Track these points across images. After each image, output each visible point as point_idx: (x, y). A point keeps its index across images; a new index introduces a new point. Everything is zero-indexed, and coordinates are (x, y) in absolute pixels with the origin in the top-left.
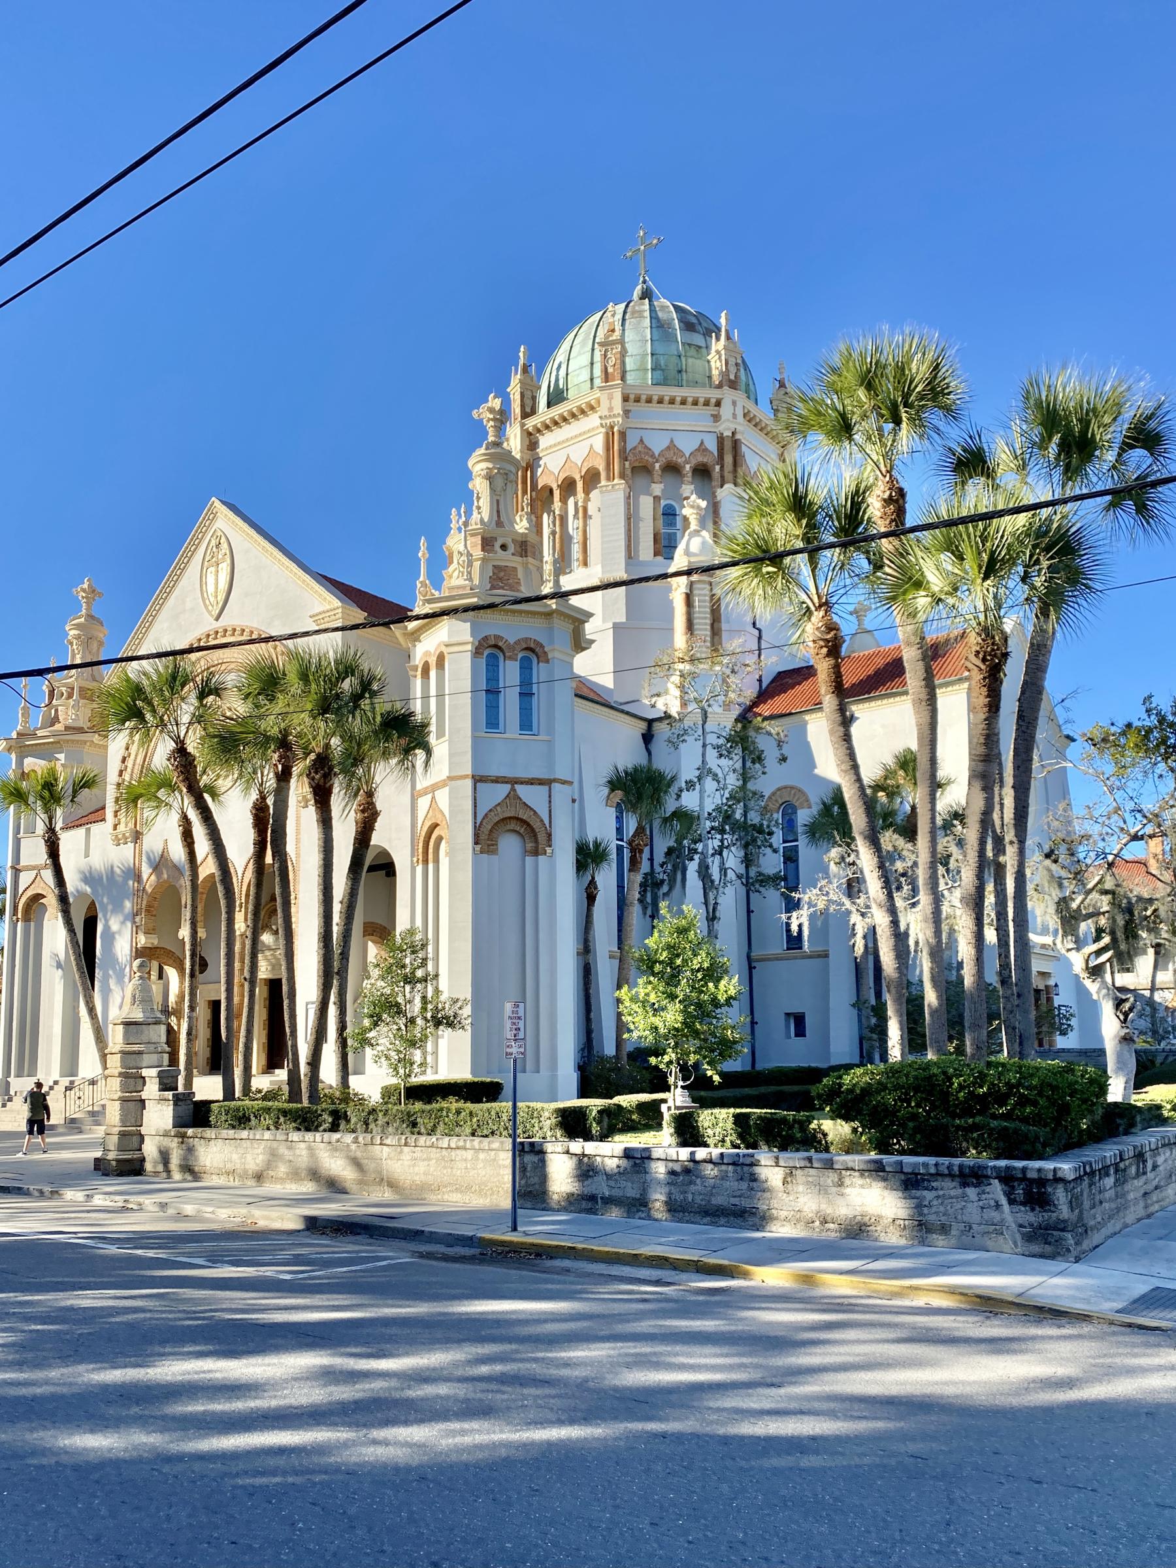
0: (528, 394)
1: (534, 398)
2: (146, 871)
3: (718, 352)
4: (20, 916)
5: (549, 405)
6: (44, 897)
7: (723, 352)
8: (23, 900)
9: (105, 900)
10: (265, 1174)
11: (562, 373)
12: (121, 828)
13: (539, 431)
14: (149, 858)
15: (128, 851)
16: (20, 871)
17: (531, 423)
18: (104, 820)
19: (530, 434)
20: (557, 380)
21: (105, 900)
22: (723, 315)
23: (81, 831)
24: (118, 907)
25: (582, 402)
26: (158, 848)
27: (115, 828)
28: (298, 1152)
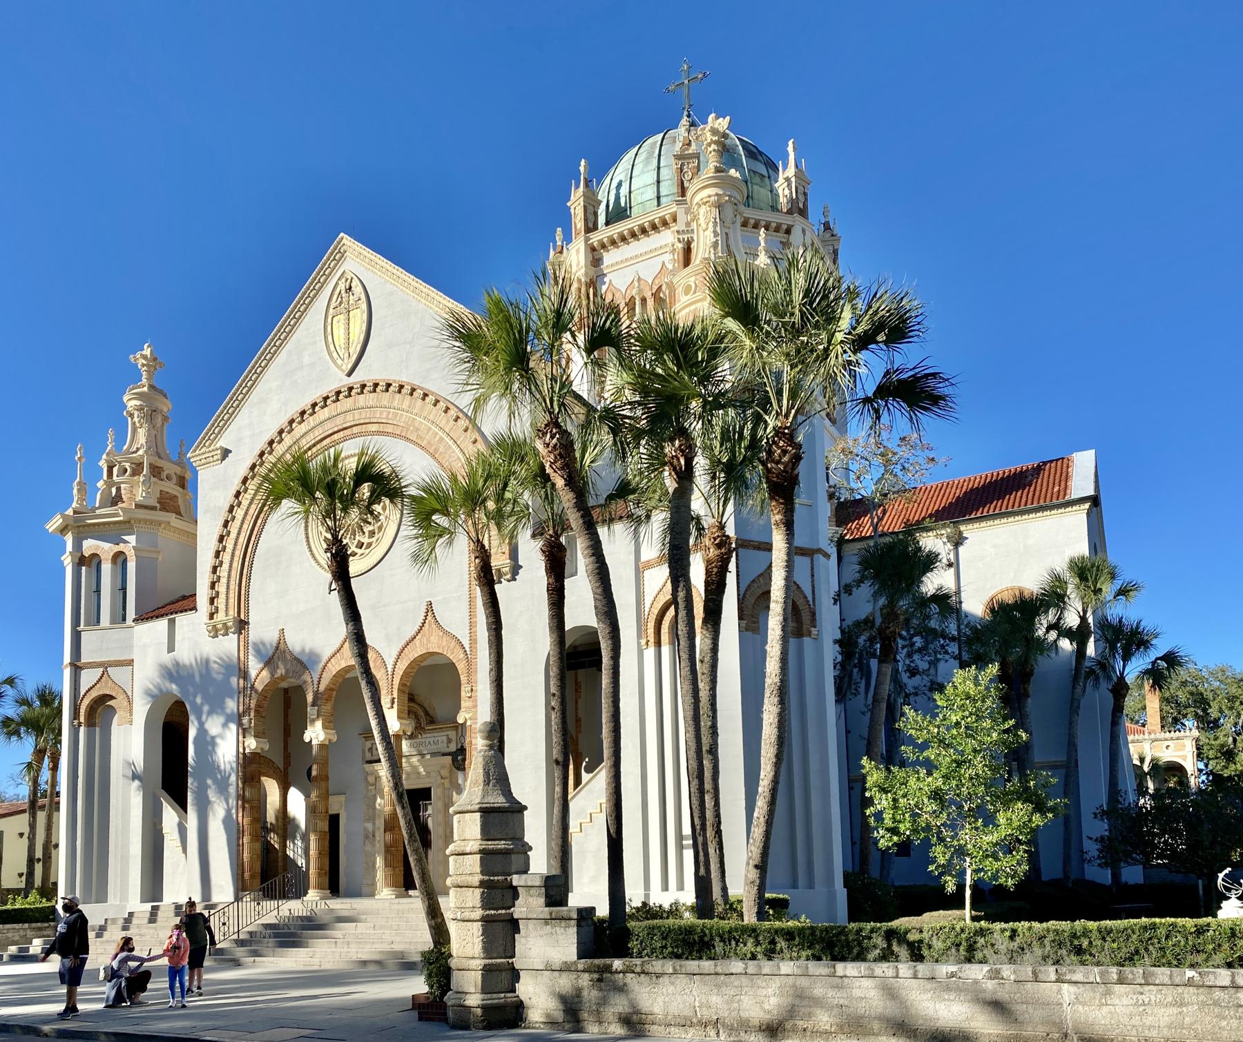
0: (591, 209)
1: (596, 214)
2: (254, 666)
3: (788, 179)
4: (82, 720)
5: (607, 223)
6: (112, 698)
7: (793, 179)
8: (86, 702)
9: (199, 700)
10: (788, 1025)
11: (624, 191)
12: (221, 616)
13: (603, 246)
14: (258, 652)
15: (229, 644)
16: (81, 668)
17: (595, 238)
18: (194, 608)
19: (593, 249)
20: (618, 198)
21: (199, 700)
22: (790, 143)
23: (163, 624)
24: (217, 707)
25: (645, 221)
26: (271, 637)
28: (857, 993)
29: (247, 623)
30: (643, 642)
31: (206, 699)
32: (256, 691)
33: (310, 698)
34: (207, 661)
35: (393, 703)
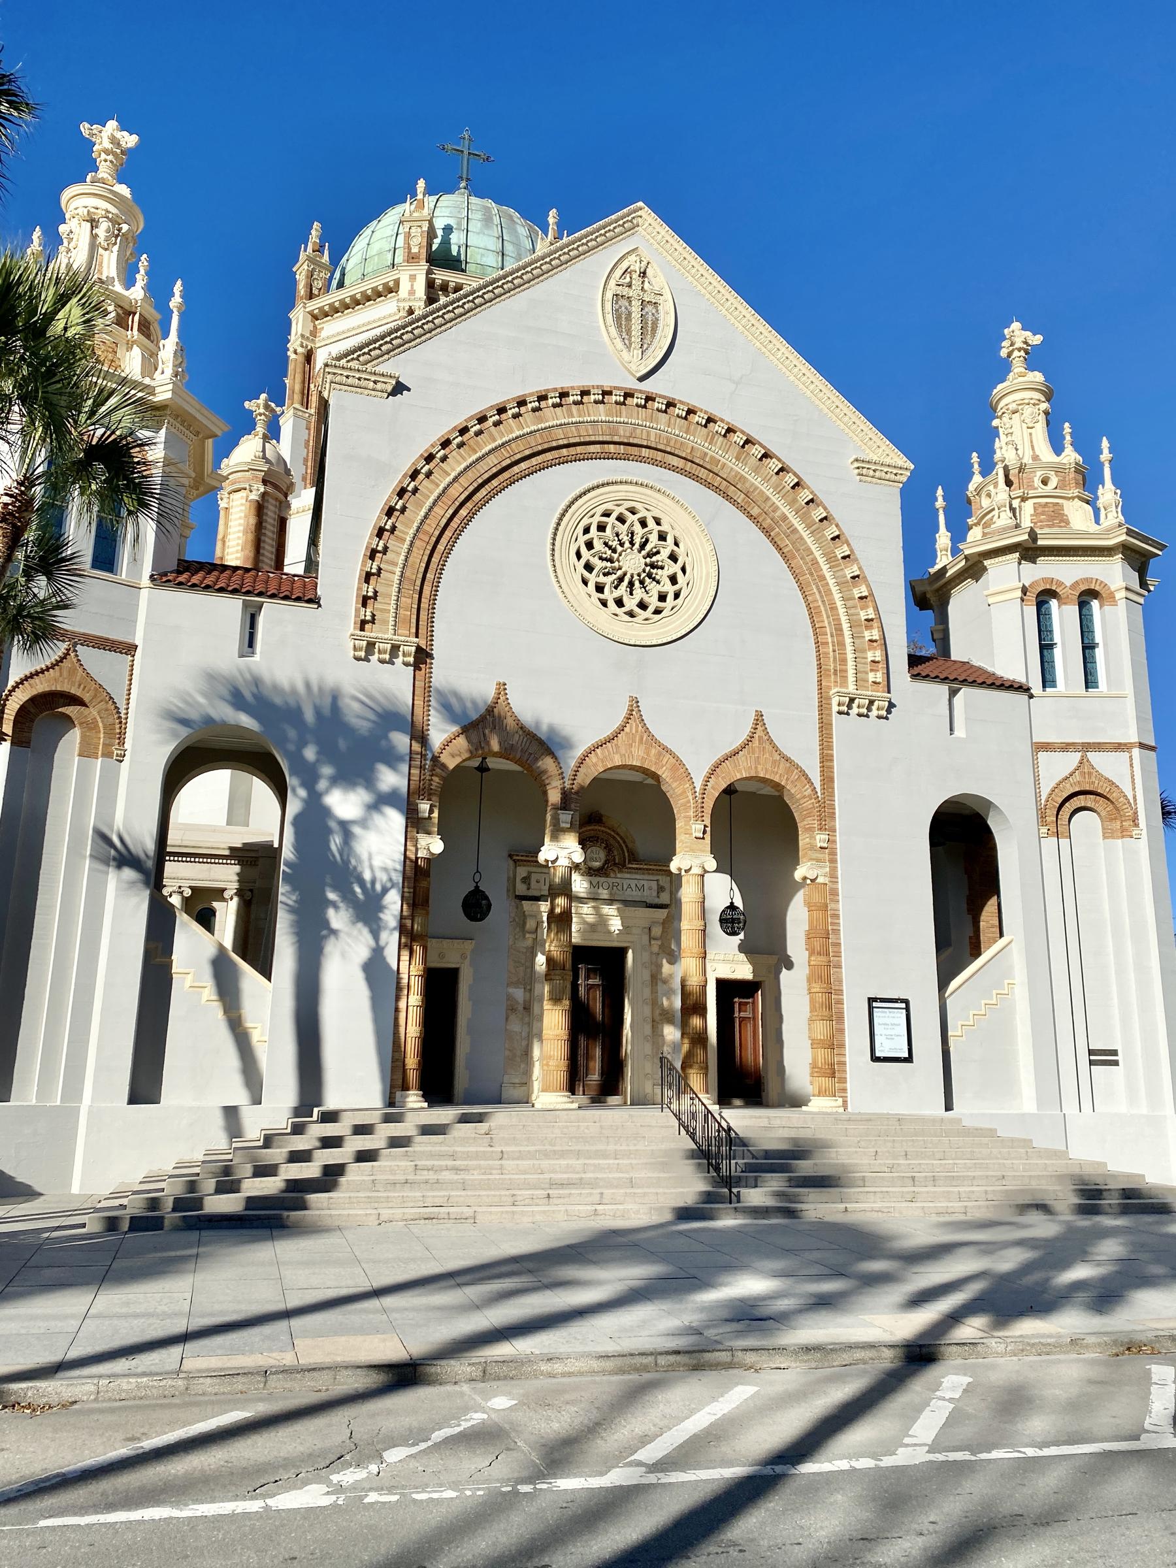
12: (384, 633)
21: (310, 753)
27: (363, 625)
29: (431, 656)
30: (1044, 830)
31: (328, 752)
32: (444, 766)
33: (554, 796)
34: (335, 697)
35: (704, 832)
